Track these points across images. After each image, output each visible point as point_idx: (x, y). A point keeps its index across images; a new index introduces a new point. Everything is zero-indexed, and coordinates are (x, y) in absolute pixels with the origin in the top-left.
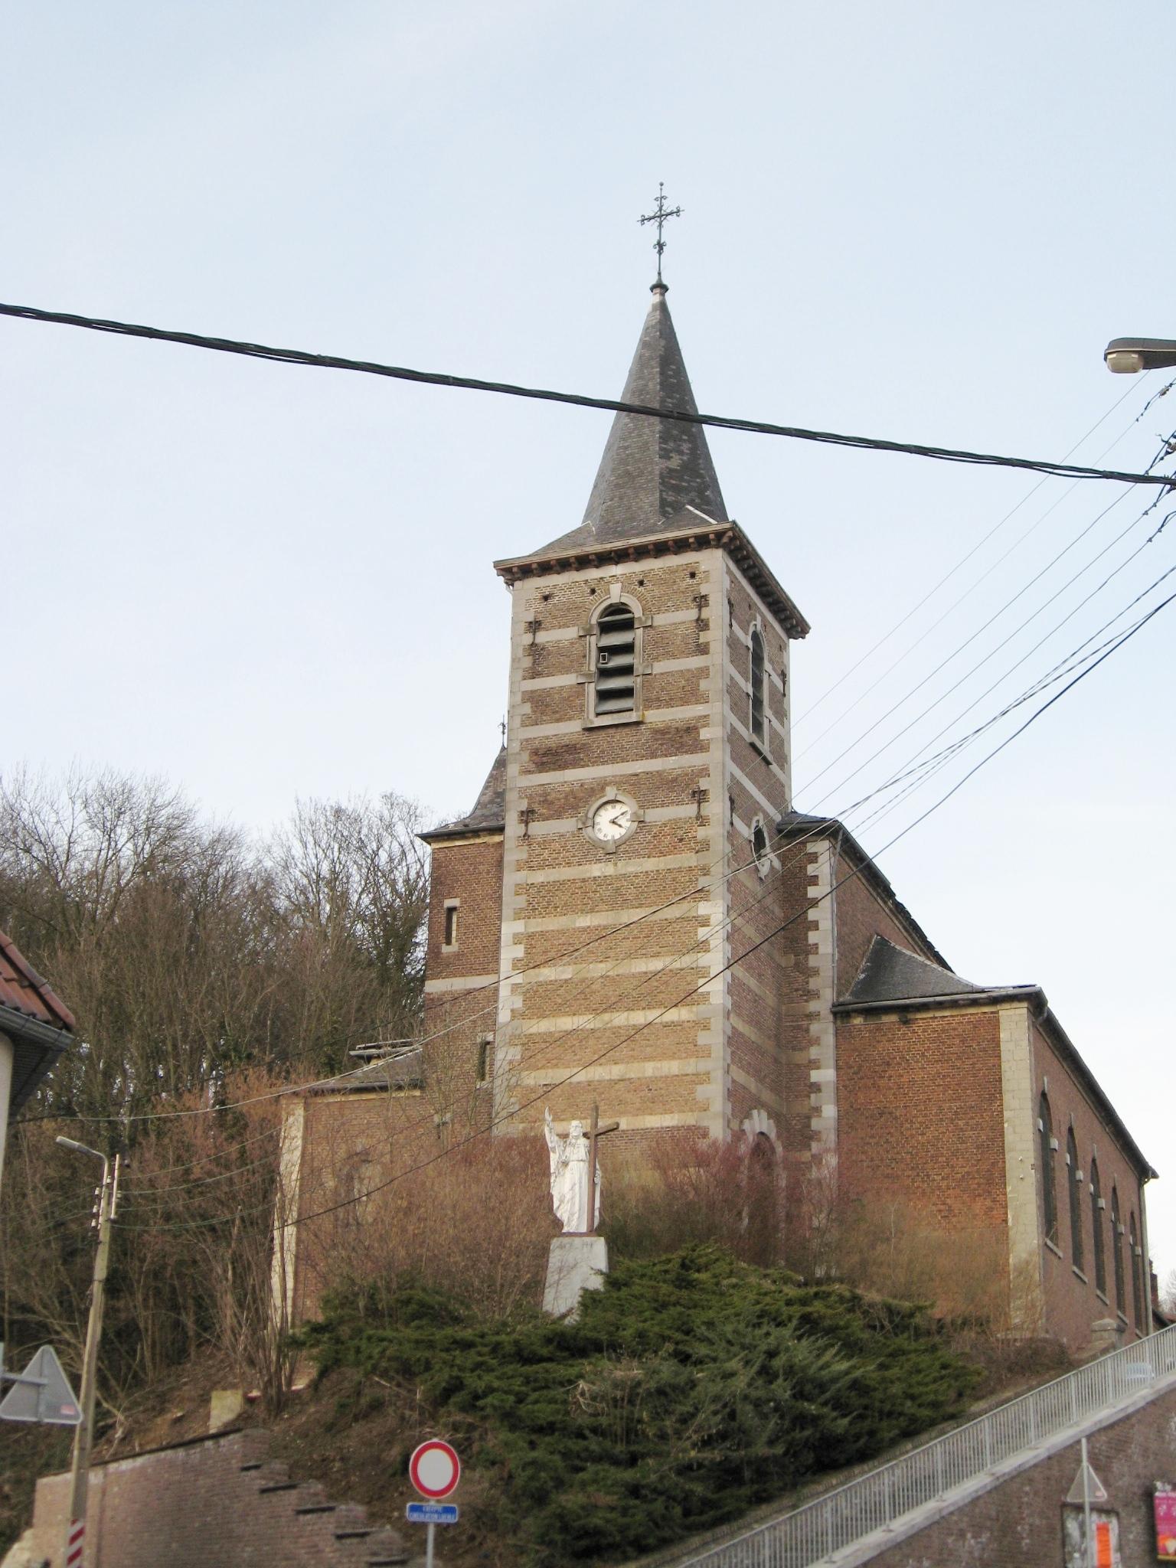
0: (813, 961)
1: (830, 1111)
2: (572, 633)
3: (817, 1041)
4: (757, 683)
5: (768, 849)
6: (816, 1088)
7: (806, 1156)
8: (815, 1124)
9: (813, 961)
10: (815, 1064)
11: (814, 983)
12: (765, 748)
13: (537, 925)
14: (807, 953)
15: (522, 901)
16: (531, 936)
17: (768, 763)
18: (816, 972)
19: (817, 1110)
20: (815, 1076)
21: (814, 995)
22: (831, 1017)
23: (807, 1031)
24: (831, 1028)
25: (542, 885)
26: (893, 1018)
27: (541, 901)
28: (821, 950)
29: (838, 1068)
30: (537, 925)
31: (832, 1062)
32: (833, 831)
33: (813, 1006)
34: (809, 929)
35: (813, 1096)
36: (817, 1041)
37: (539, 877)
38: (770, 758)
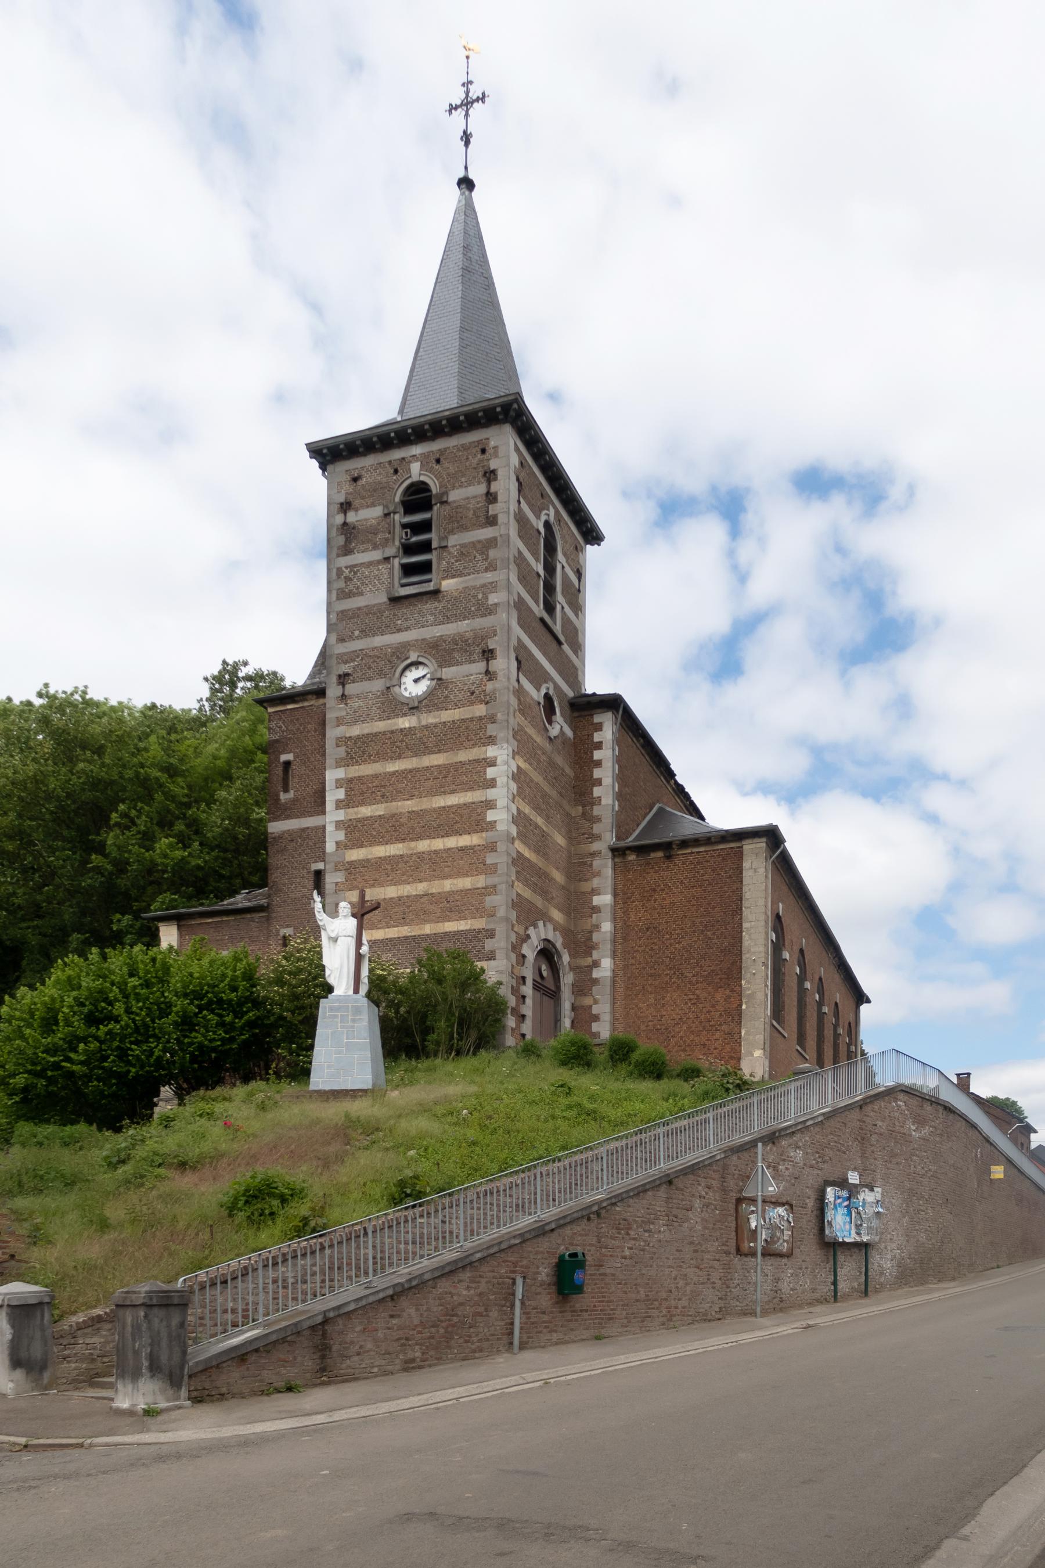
0: (596, 811)
1: (607, 927)
2: (377, 511)
3: (598, 874)
4: (550, 569)
5: (558, 716)
6: (596, 910)
7: (589, 961)
8: (595, 937)
9: (596, 811)
10: (595, 892)
11: (597, 829)
12: (558, 628)
13: (355, 771)
14: (593, 804)
15: (342, 751)
16: (350, 781)
17: (560, 643)
18: (598, 819)
19: (597, 927)
20: (596, 900)
21: (594, 838)
22: (610, 854)
23: (591, 865)
24: (610, 863)
25: (358, 737)
26: (660, 854)
27: (359, 750)
28: (604, 802)
29: (615, 895)
30: (355, 771)
31: (609, 889)
32: (614, 703)
33: (596, 846)
34: (594, 785)
35: (594, 916)
36: (598, 874)
37: (356, 731)
38: (562, 638)
